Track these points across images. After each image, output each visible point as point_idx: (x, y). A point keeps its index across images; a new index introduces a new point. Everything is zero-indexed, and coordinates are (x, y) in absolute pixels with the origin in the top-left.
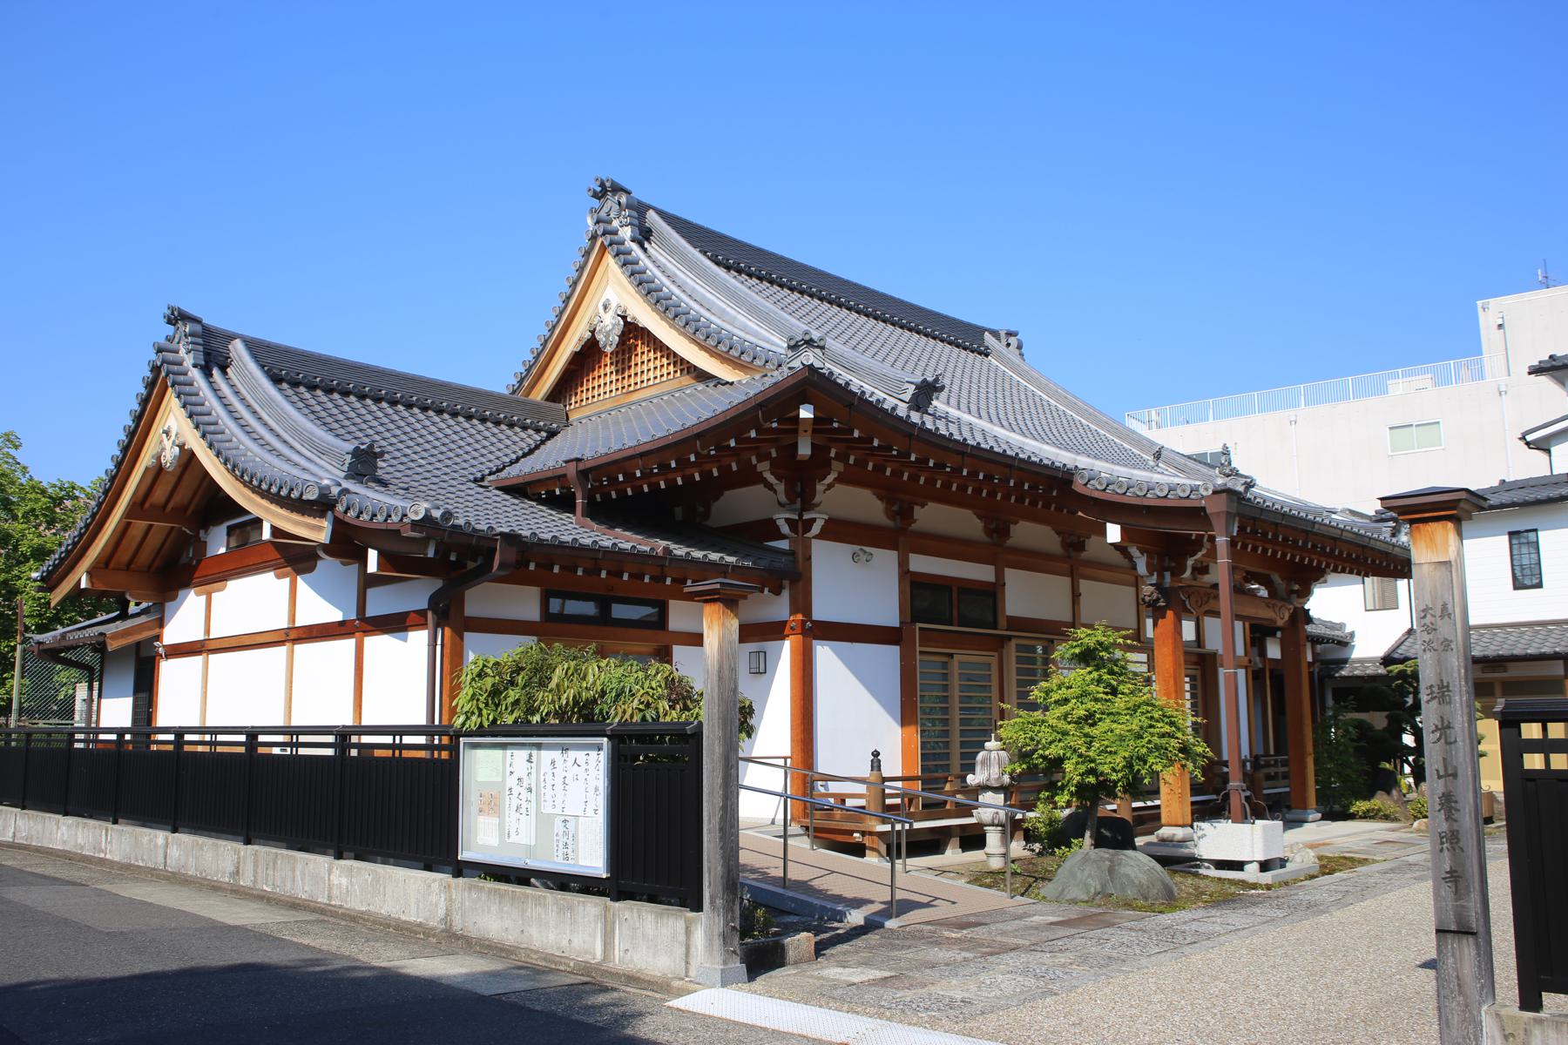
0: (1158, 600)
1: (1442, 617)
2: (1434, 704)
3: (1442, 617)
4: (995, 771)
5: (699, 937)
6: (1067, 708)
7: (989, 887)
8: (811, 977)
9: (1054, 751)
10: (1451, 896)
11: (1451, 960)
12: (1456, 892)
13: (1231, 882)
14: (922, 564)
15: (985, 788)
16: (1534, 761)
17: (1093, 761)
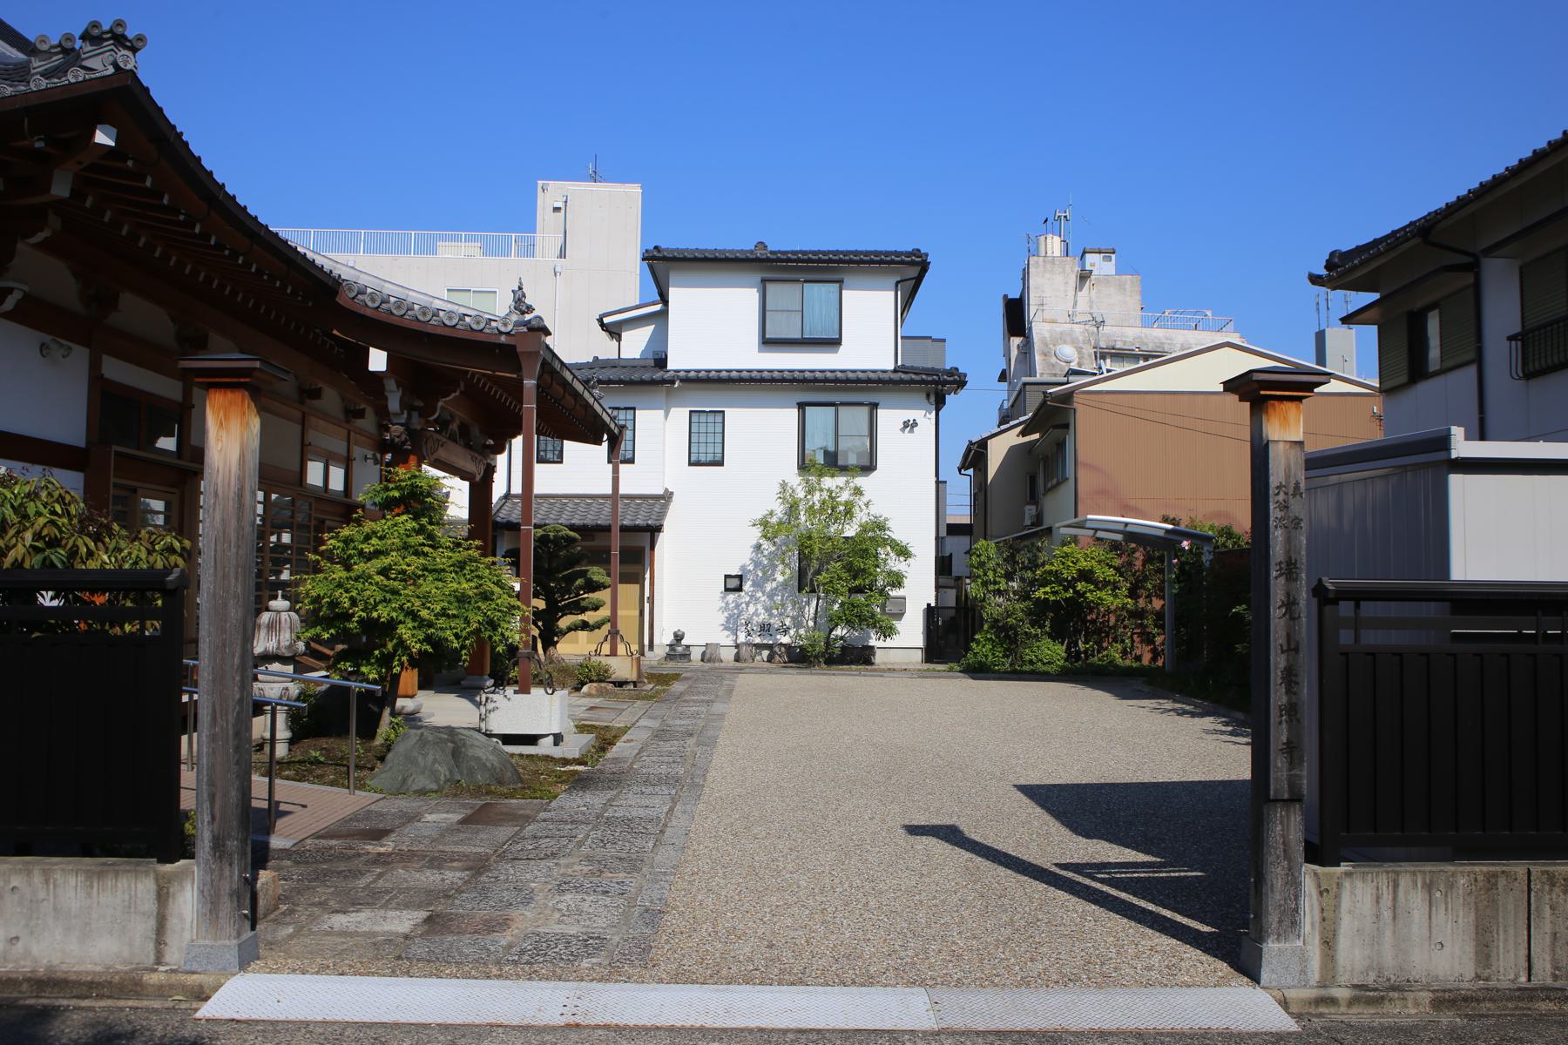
0: (404, 443)
1: (1294, 495)
2: (1282, 580)
3: (1294, 495)
4: (286, 637)
5: (187, 902)
6: (386, 561)
7: (332, 784)
8: (330, 932)
9: (383, 613)
10: (1286, 766)
11: (1279, 828)
12: (1291, 763)
13: (530, 756)
14: (116, 370)
15: (268, 658)
16: (1346, 637)
17: (430, 625)
